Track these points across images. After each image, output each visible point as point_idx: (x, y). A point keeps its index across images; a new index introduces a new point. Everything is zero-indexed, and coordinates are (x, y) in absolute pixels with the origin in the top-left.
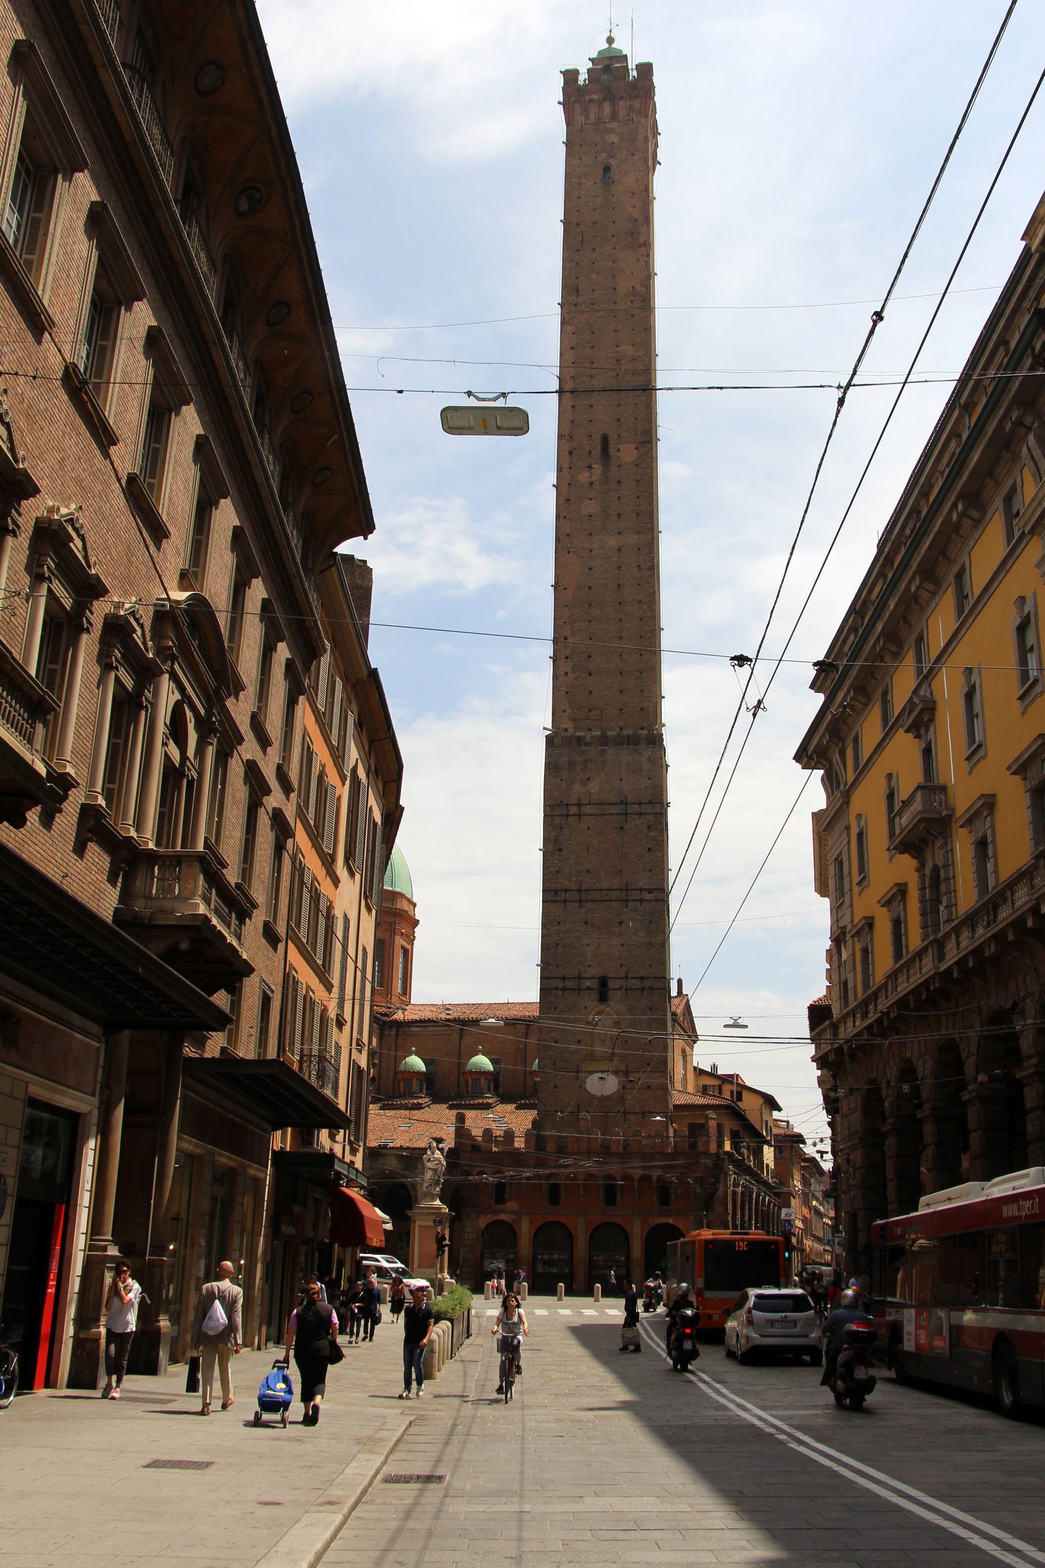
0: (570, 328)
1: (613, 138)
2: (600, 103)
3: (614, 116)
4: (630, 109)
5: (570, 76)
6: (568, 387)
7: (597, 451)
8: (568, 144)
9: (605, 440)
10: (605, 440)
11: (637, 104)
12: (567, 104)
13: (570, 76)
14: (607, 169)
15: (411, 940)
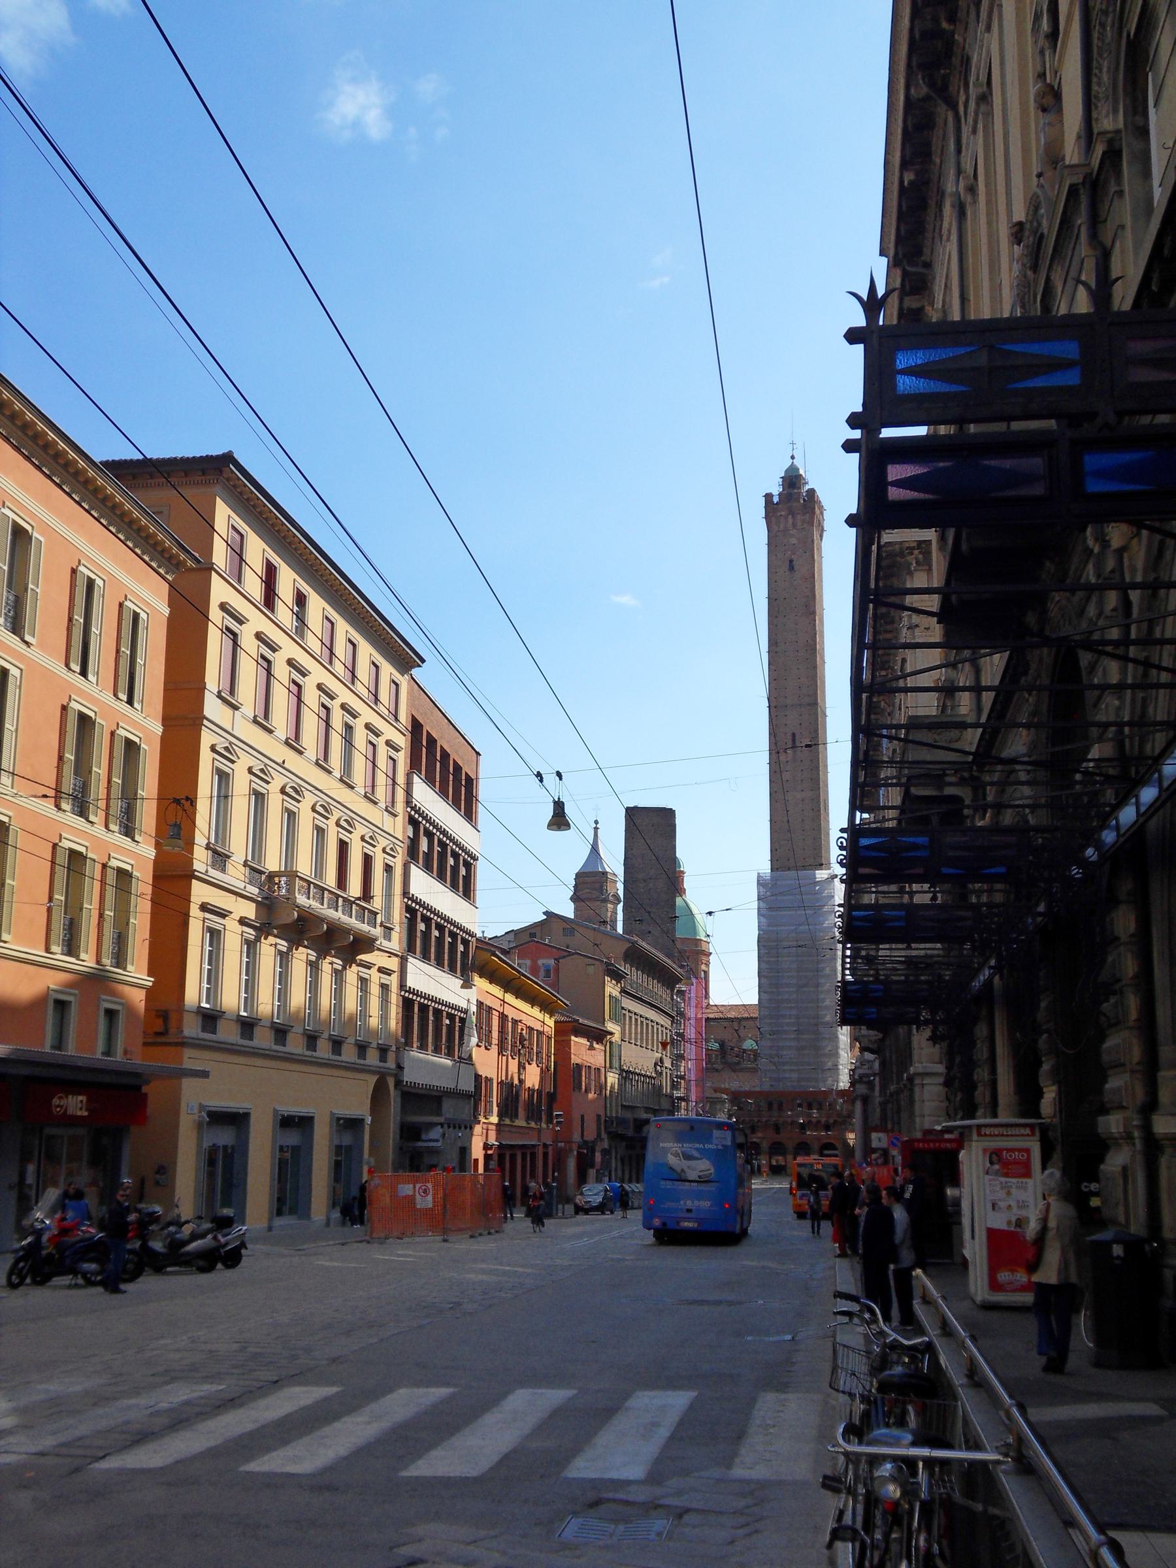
0: (773, 667)
1: (793, 541)
2: (786, 518)
3: (794, 525)
4: (803, 521)
5: (768, 497)
6: (773, 705)
7: (790, 744)
8: (769, 544)
9: (794, 735)
10: (794, 735)
11: (807, 517)
12: (767, 517)
13: (768, 497)
14: (791, 561)
15: (708, 965)
